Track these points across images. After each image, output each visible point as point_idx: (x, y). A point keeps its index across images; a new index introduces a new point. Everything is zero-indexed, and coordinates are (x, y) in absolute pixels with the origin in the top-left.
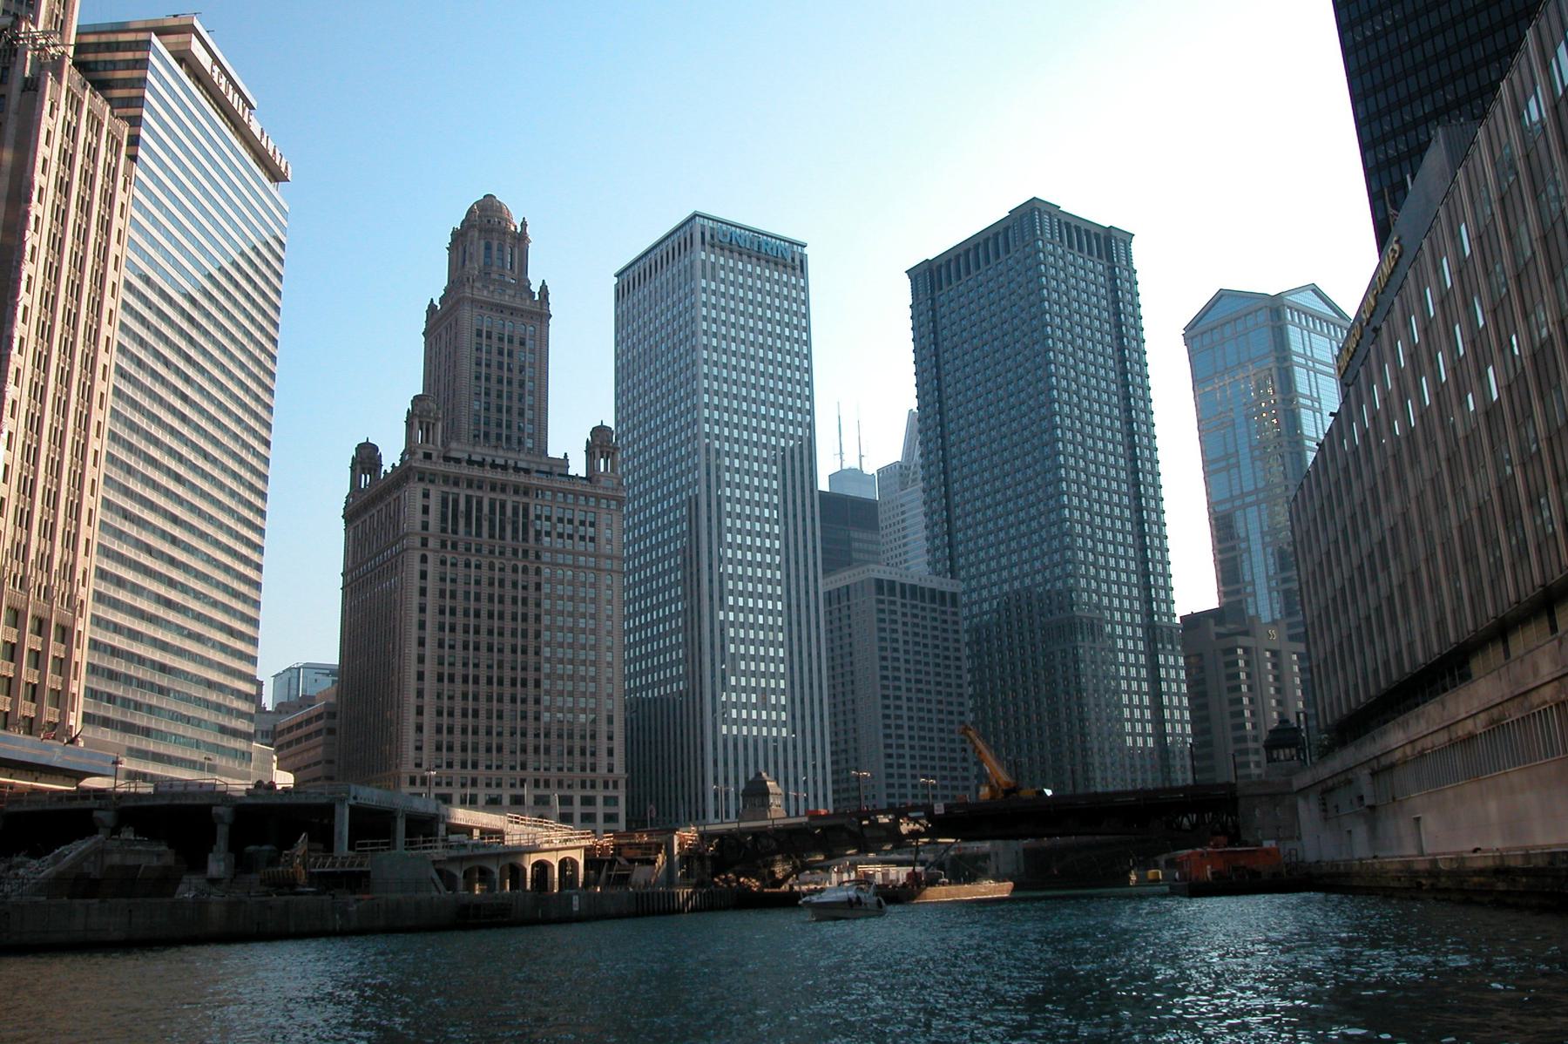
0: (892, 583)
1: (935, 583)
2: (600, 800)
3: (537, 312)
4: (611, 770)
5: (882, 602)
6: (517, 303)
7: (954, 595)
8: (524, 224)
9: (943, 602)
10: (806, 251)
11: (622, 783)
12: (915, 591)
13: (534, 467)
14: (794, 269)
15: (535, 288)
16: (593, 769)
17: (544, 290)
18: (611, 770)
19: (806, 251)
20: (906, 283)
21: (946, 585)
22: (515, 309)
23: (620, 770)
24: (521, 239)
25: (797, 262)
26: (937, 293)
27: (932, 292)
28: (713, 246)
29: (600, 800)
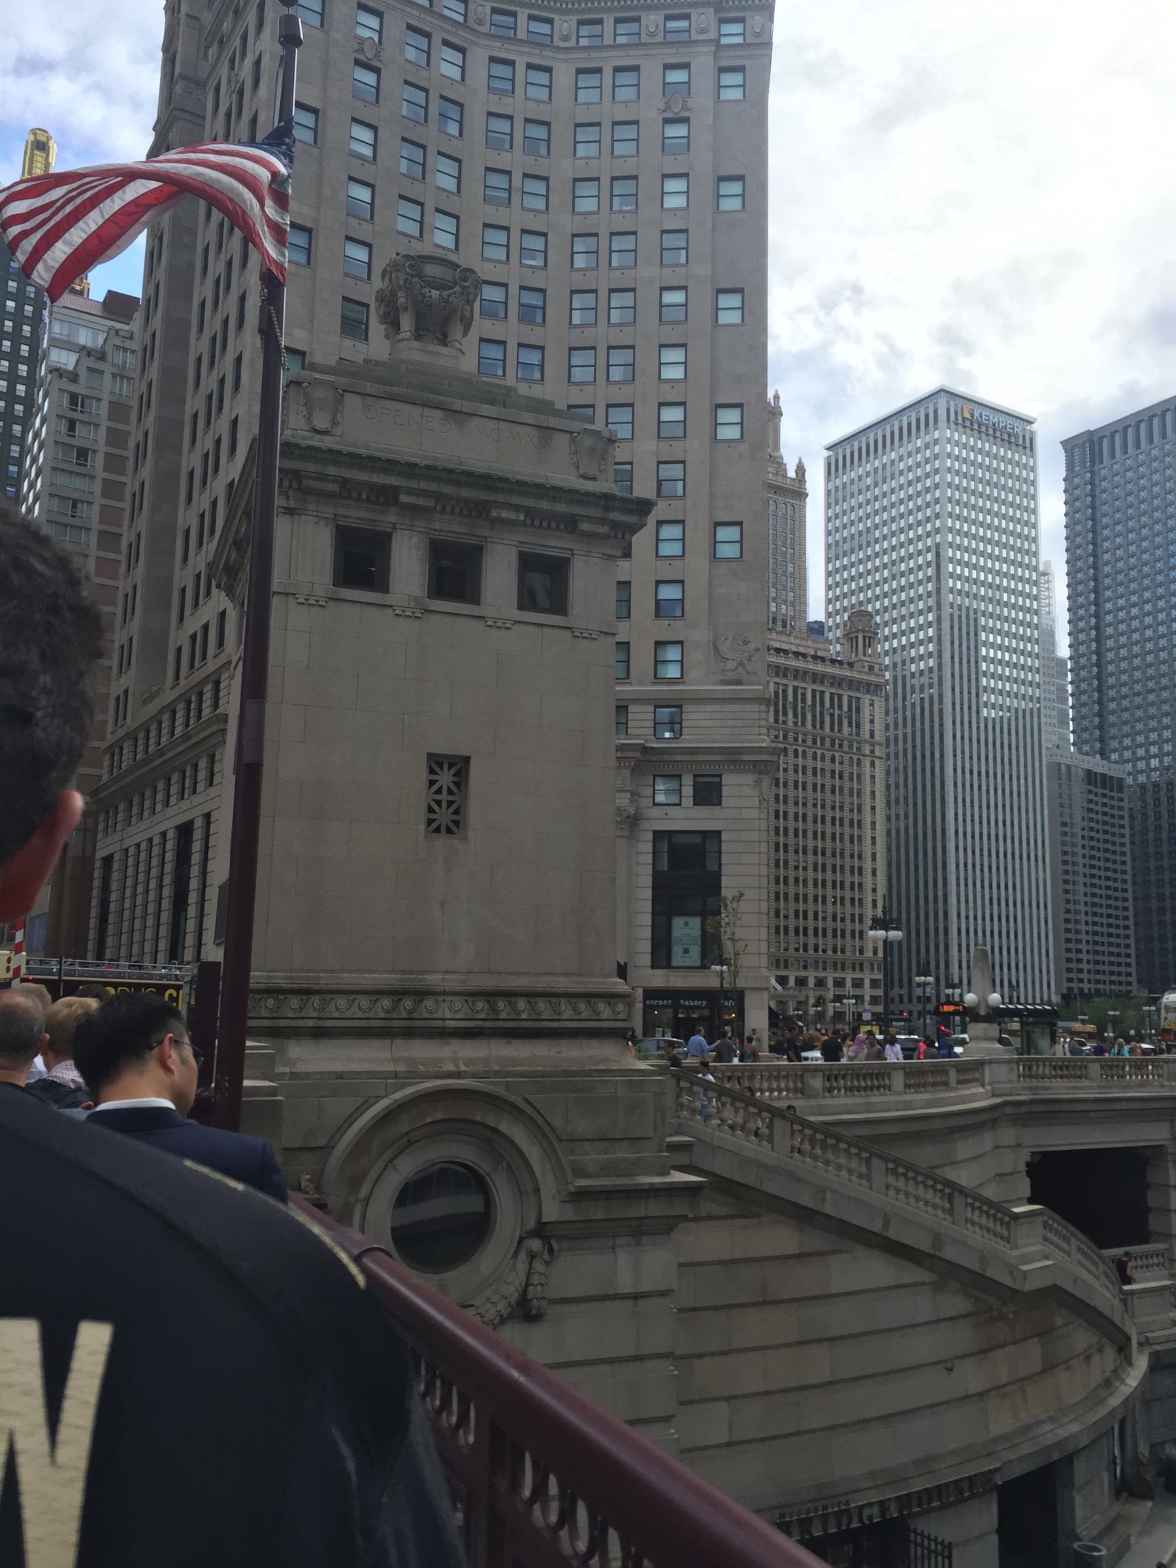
2: (867, 983)
3: (797, 492)
6: (779, 482)
10: (1034, 427)
13: (802, 650)
14: (1025, 448)
16: (861, 952)
19: (1034, 427)
22: (780, 488)
25: (1028, 444)
26: (1097, 467)
27: (1092, 465)
28: (957, 424)
29: (867, 983)
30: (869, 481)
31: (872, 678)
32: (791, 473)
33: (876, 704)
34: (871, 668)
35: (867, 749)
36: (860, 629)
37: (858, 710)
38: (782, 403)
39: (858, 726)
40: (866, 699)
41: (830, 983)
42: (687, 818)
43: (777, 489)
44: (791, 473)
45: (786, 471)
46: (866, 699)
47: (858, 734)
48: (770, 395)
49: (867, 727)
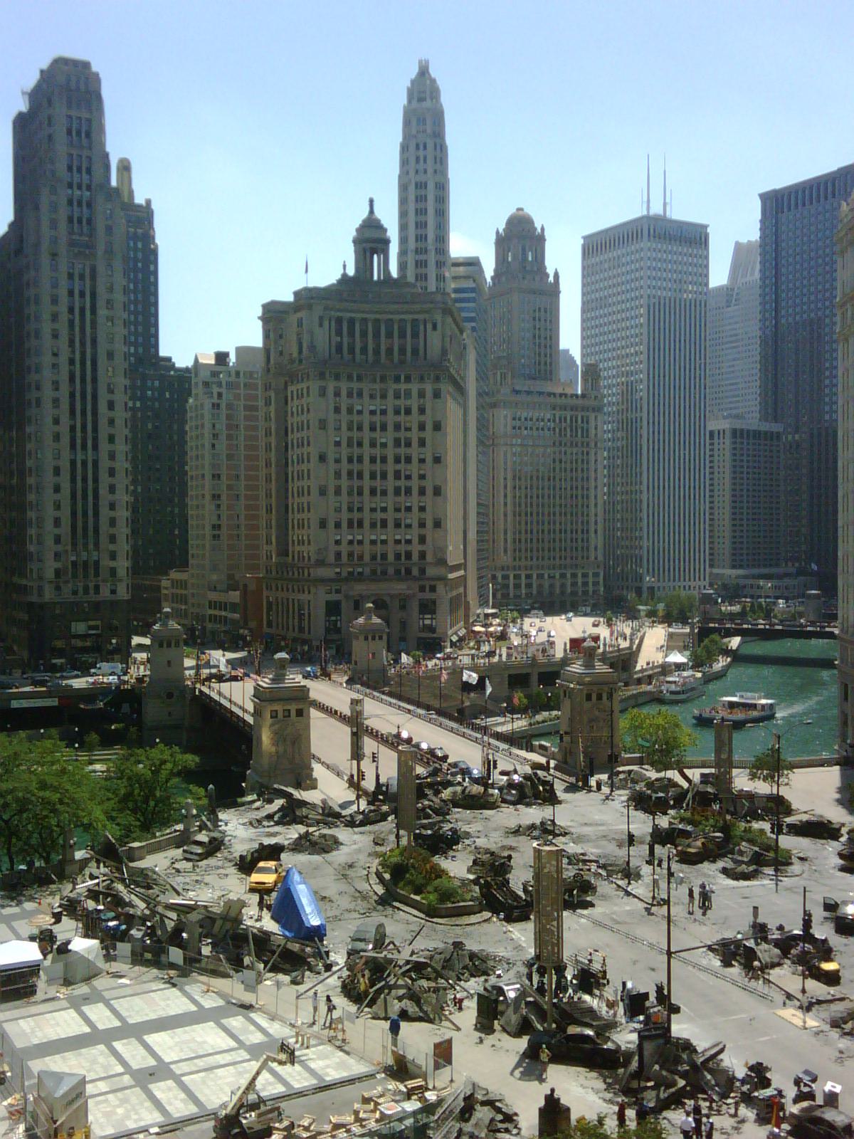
0: (742, 430)
1: (765, 427)
3: (553, 292)
4: (596, 558)
5: (735, 443)
7: (778, 433)
8: (543, 229)
9: (772, 439)
11: (602, 567)
12: (757, 434)
15: (550, 271)
17: (556, 275)
18: (596, 558)
19: (709, 230)
20: (758, 204)
21: (776, 427)
23: (600, 558)
24: (541, 239)
30: (606, 266)
31: (596, 403)
32: (551, 279)
33: (599, 418)
34: (596, 397)
35: (592, 445)
36: (591, 372)
37: (587, 422)
38: (546, 233)
39: (587, 431)
40: (592, 416)
41: (569, 576)
42: (428, 595)
43: (541, 293)
44: (551, 279)
45: (548, 276)
46: (592, 416)
47: (587, 437)
48: (539, 230)
49: (593, 432)
